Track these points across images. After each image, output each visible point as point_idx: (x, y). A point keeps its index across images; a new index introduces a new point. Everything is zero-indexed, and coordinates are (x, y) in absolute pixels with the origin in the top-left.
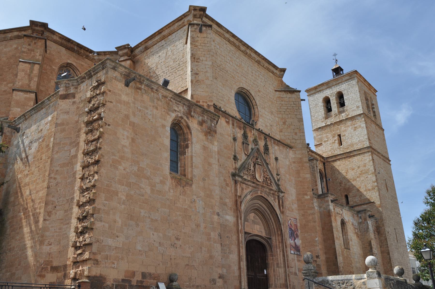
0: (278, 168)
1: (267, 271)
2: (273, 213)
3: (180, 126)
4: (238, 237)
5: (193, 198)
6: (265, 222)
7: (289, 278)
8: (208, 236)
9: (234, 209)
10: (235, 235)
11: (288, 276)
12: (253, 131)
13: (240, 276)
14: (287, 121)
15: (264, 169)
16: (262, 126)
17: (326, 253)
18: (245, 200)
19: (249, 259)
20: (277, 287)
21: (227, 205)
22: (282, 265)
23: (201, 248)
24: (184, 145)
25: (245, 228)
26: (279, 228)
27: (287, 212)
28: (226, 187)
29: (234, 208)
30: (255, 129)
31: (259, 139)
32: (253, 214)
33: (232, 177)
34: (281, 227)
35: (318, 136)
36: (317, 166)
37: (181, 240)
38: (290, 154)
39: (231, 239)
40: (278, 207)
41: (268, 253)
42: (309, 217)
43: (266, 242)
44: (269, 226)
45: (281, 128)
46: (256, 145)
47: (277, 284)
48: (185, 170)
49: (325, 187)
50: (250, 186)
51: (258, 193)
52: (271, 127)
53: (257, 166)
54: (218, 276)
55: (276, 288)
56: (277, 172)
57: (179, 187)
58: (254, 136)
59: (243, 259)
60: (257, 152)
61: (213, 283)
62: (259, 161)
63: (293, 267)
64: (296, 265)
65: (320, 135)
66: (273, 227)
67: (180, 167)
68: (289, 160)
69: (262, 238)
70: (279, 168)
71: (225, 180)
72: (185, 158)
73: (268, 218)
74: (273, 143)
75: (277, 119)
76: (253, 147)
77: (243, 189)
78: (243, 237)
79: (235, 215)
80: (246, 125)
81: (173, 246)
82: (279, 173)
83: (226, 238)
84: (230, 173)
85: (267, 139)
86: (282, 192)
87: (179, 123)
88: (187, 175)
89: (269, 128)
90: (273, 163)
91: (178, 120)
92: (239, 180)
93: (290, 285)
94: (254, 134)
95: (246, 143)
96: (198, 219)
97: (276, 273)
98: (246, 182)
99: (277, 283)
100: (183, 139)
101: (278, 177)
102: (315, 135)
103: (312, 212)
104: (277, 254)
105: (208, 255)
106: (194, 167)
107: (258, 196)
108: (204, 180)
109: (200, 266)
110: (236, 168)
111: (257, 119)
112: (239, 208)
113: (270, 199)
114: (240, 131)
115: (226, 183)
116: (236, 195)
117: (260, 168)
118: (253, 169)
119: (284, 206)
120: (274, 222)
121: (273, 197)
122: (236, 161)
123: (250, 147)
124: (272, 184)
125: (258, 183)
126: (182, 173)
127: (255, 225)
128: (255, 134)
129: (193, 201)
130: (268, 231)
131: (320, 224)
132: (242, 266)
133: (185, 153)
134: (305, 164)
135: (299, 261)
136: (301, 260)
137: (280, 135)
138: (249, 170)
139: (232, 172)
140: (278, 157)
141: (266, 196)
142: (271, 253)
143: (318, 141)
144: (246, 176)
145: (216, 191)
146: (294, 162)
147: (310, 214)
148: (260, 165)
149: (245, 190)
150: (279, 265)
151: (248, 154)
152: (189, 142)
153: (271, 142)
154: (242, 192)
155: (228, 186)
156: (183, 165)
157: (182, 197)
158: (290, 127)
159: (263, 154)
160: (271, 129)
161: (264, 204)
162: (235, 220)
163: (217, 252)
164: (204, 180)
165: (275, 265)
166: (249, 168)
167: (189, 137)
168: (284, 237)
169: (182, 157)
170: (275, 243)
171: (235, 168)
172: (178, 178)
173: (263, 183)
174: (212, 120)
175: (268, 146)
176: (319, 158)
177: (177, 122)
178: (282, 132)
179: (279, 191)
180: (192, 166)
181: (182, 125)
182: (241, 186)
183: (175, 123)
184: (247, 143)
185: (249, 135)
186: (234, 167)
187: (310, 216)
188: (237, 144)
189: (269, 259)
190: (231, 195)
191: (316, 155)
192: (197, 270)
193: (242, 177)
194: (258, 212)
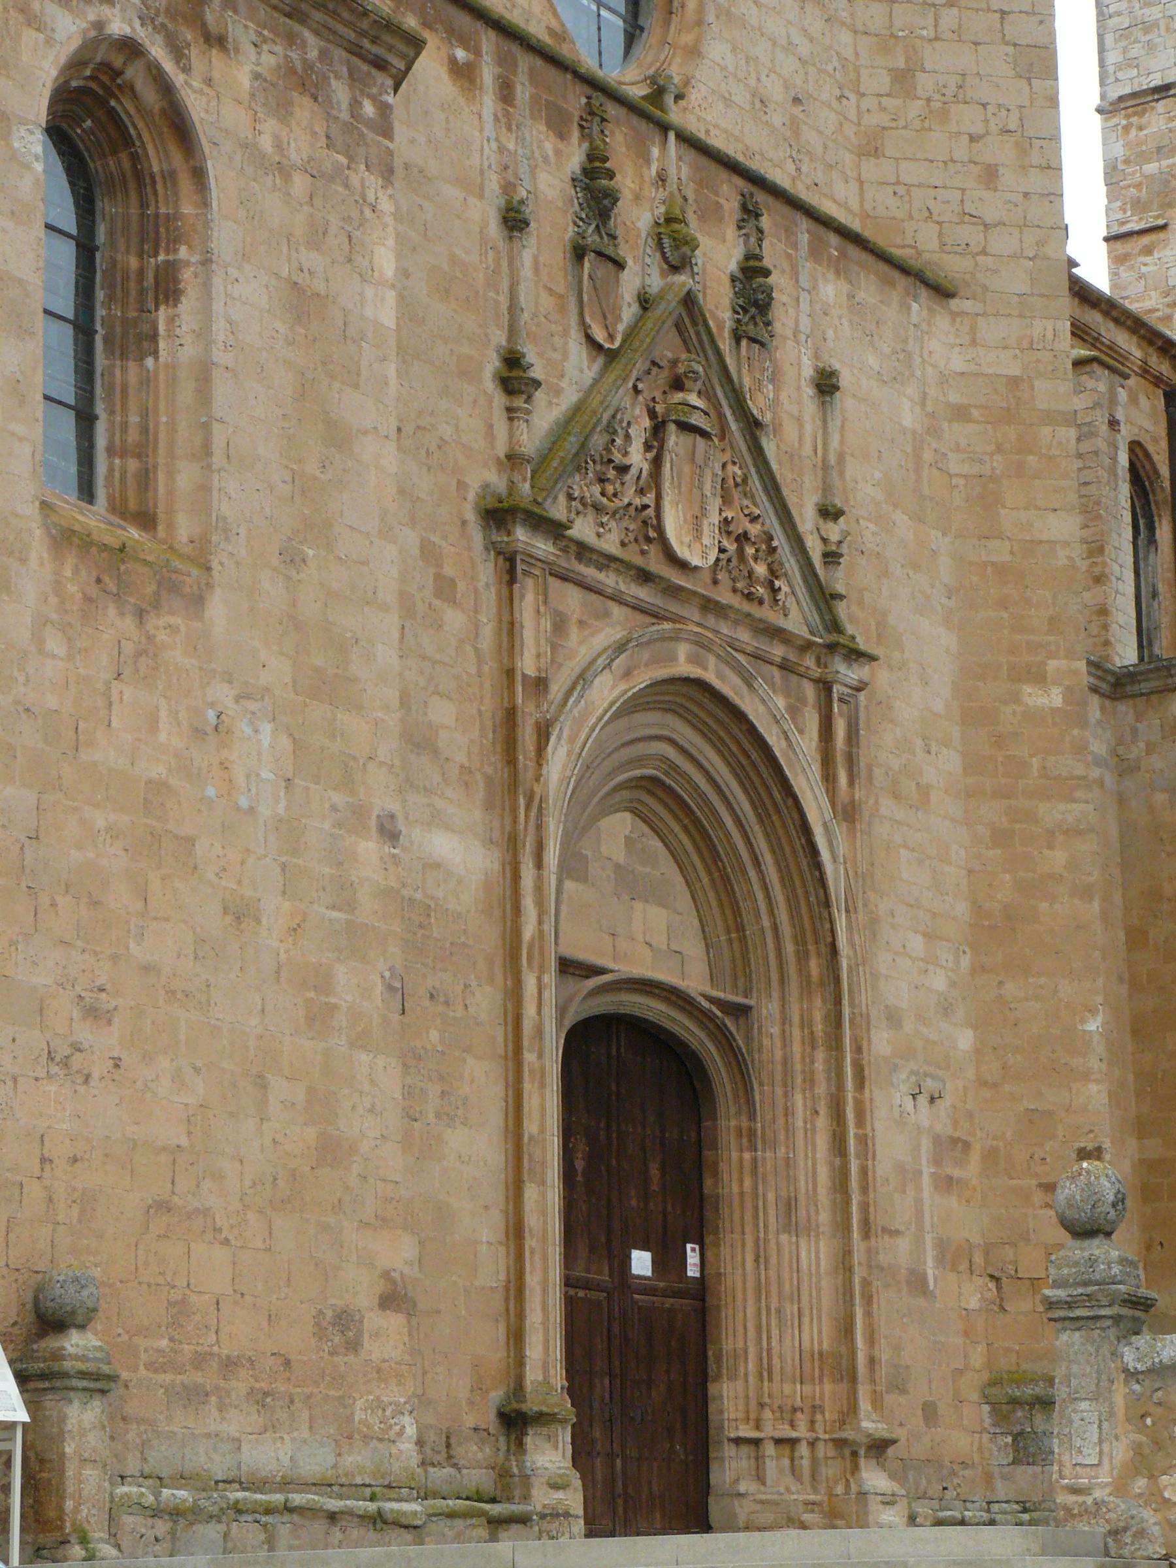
0: (832, 459)
1: (709, 1254)
2: (778, 812)
3: (113, 115)
4: (515, 995)
5: (212, 705)
6: (712, 881)
7: (868, 1314)
8: (312, 994)
9: (489, 781)
10: (491, 980)
11: (863, 1295)
12: (655, 152)
13: (516, 1289)
14: (928, 67)
15: (724, 466)
16: (728, 101)
17: (1142, 1128)
18: (574, 708)
19: (580, 1165)
20: (776, 1377)
21: (436, 752)
22: (824, 1217)
23: (261, 1083)
24: (141, 272)
25: (563, 925)
26: (815, 932)
27: (883, 811)
28: (437, 603)
29: (490, 770)
30: (672, 136)
31: (702, 217)
32: (628, 816)
33: (486, 528)
34: (832, 922)
35: (1143, 158)
36: (1113, 424)
37: (116, 1020)
38: (934, 345)
39: (460, 1013)
40: (816, 769)
41: (722, 1123)
42: (1046, 852)
43: (710, 1034)
44: (737, 912)
45: (876, 119)
46: (675, 269)
47: (775, 1351)
48: (145, 480)
49: (1162, 588)
50: (618, 599)
51: (673, 659)
52: (797, 110)
53: (674, 439)
54: (380, 1287)
55: (770, 1380)
56: (826, 489)
57: (112, 611)
58: (662, 194)
59: (543, 1163)
60: (679, 327)
61: (337, 1339)
62: (694, 399)
63: (897, 1233)
64: (927, 1216)
65: (1159, 149)
66: (766, 922)
67: (110, 451)
68: (925, 395)
69: (682, 1009)
70: (841, 458)
71: (429, 552)
72: (146, 382)
73: (739, 857)
74: (804, 251)
75: (846, 37)
76: (656, 282)
77: (560, 625)
78: (546, 994)
79: (496, 824)
80: (603, 99)
81: (65, 1063)
82: (838, 502)
83: (427, 1003)
84: (471, 496)
85: (765, 222)
86: (856, 655)
87: (108, 90)
88: (161, 516)
89: (777, 119)
90: (799, 420)
91: (106, 66)
92: (540, 554)
93: (872, 1361)
94: (662, 178)
95: (600, 254)
96: (243, 863)
97: (772, 1273)
98: (589, 572)
99: (774, 1343)
100: (135, 227)
101: (833, 531)
102: (1119, 150)
103: (1070, 818)
104: (789, 1130)
105: (311, 1132)
106: (218, 460)
107: (673, 680)
108: (292, 559)
109: (251, 1216)
110: (513, 459)
111: (688, 38)
112: (530, 774)
113: (761, 708)
114: (561, 146)
115: (438, 577)
116: (510, 673)
117: (699, 458)
118: (646, 467)
119: (862, 765)
120: (784, 886)
121: (787, 695)
122: (519, 402)
123: (630, 283)
124: (785, 589)
125: (677, 579)
126: (124, 500)
127: (638, 906)
128: (672, 173)
129: (210, 729)
130: (726, 953)
131: (1118, 899)
132: (531, 1220)
133: (154, 337)
134: (1046, 431)
135: (946, 1184)
136: (959, 1180)
137: (861, 183)
138: (611, 474)
139: (486, 487)
140: (837, 366)
141: (729, 685)
142: (745, 1124)
143: (1138, 205)
145: (380, 646)
146: (961, 414)
147: (1051, 833)
148: (704, 434)
149: (574, 633)
150: (802, 1213)
151: (611, 337)
152: (183, 252)
153: (795, 245)
154: (554, 647)
155: (452, 600)
156: (133, 436)
157: (128, 692)
158: (943, 116)
159: (725, 344)
160: (797, 132)
161: (709, 740)
162: (497, 866)
163: (371, 1110)
164: (292, 559)
165: (772, 1212)
166: (617, 457)
167: (187, 209)
168: (852, 1005)
169: (124, 370)
170: (778, 1043)
171: (509, 457)
172: (104, 547)
173: (715, 582)
174: (365, 67)
175: (766, 273)
176: (1137, 353)
177: (92, 78)
178: (876, 152)
179: (832, 647)
180: (206, 449)
181: (132, 111)
182: (545, 602)
183: (78, 90)
184: (610, 251)
185: (626, 182)
186: (501, 450)
187: (1051, 847)
188: (527, 257)
189: (723, 1167)
191: (1111, 325)
192: (226, 1242)
193: (556, 530)
194: (666, 805)
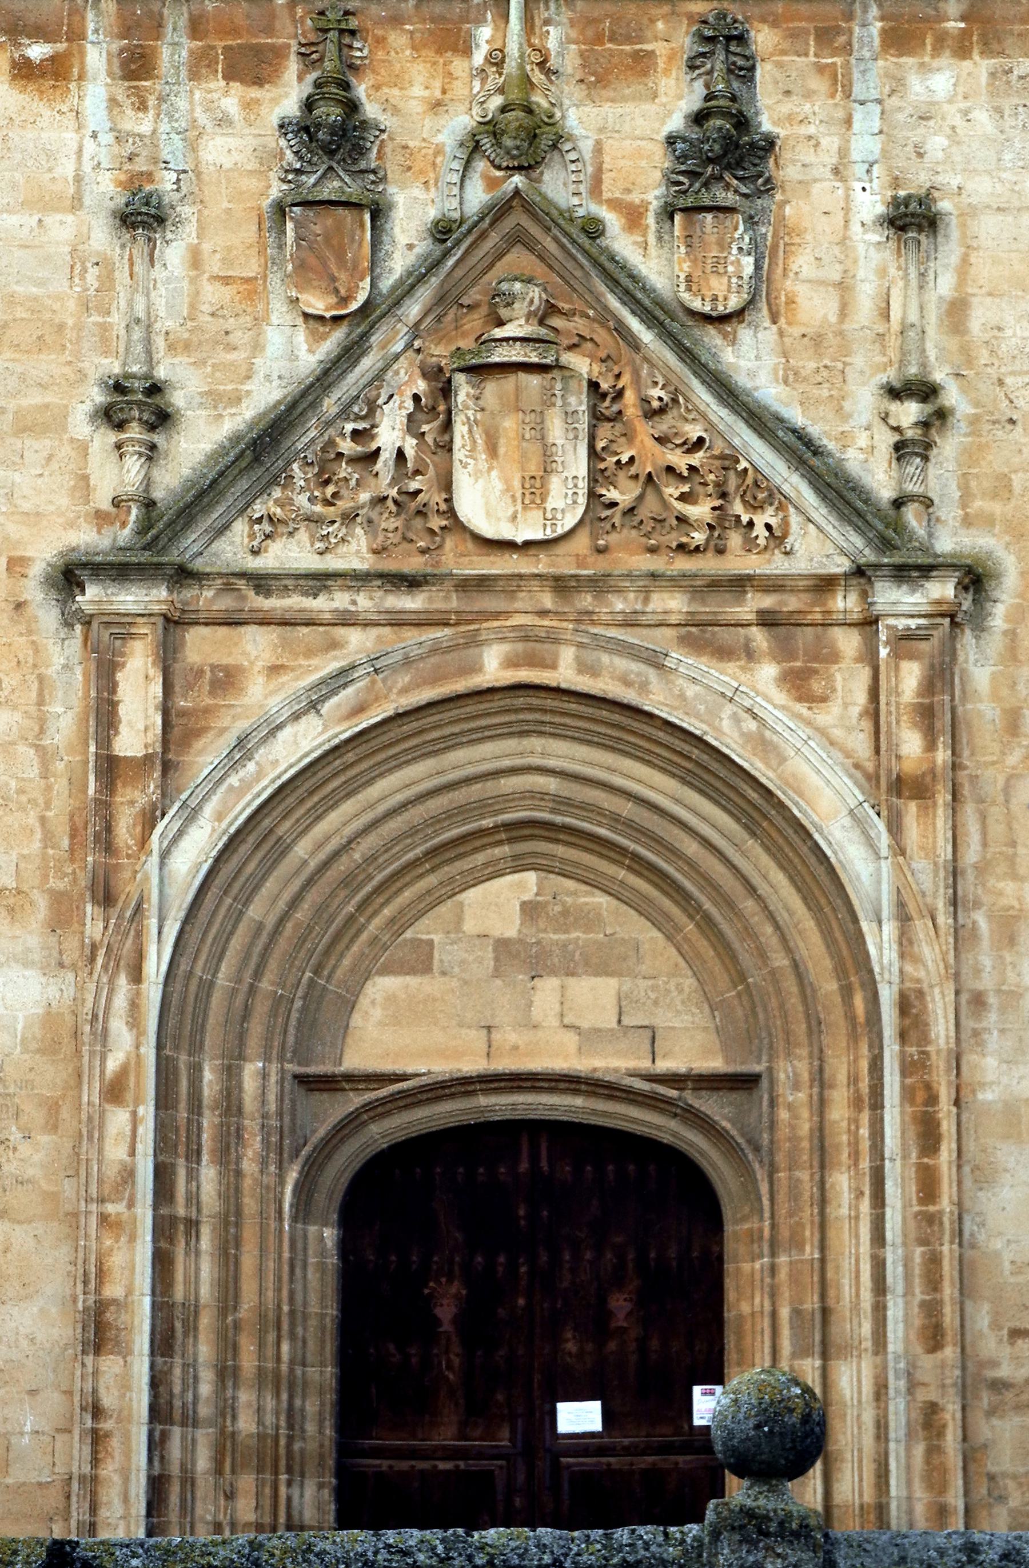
2: (765, 817)
50: (346, 620)
51: (476, 668)
144: (303, 535)
190: (33, 772)
